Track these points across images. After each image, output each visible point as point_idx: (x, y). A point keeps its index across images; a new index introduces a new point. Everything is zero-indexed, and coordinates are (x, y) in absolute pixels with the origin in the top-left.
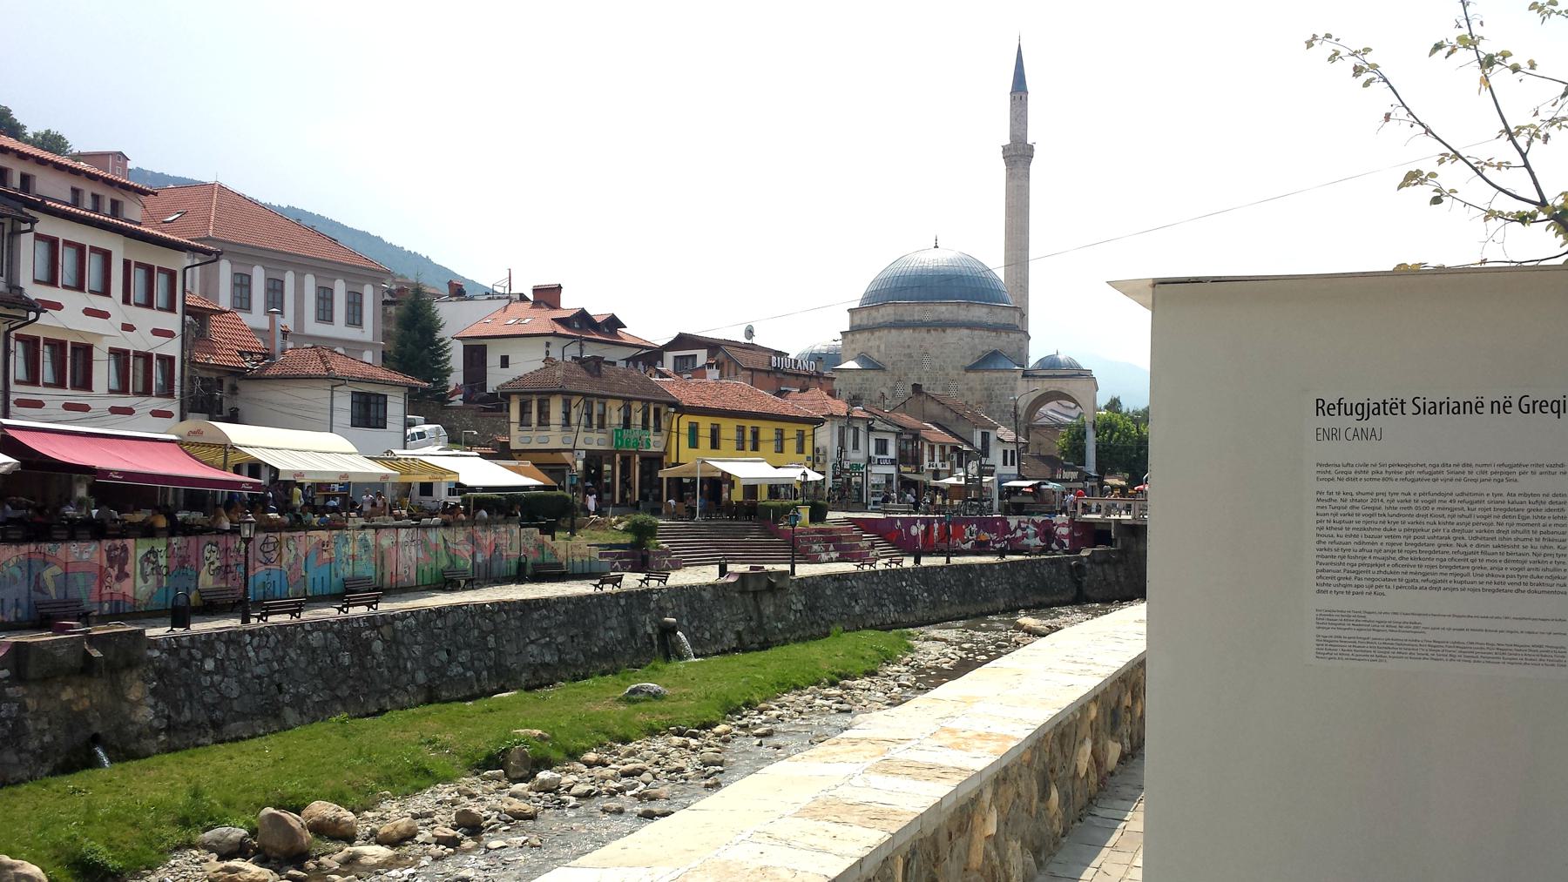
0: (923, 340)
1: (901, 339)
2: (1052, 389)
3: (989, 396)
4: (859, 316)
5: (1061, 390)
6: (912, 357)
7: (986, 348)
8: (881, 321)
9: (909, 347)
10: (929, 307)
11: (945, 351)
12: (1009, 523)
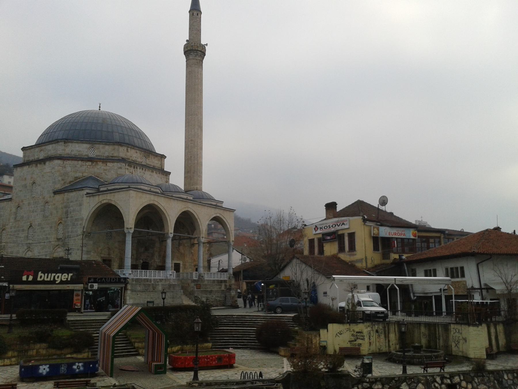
1: (22, 174)
2: (105, 202)
3: (67, 213)
5: (110, 202)
6: (27, 187)
7: (79, 175)
10: (43, 147)
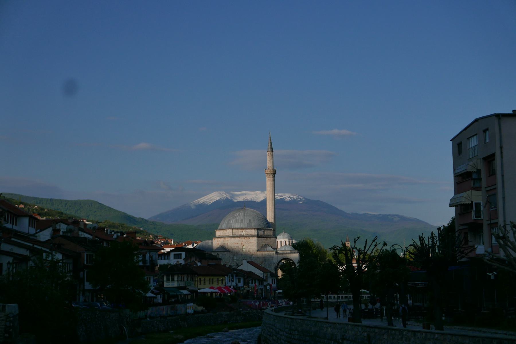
0: (242, 241)
1: (235, 241)
4: (219, 232)
6: (239, 247)
7: (263, 243)
8: (228, 234)
9: (238, 244)
11: (249, 245)
12: (278, 302)
